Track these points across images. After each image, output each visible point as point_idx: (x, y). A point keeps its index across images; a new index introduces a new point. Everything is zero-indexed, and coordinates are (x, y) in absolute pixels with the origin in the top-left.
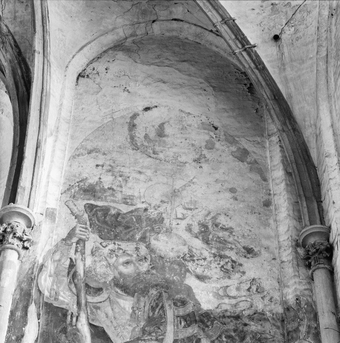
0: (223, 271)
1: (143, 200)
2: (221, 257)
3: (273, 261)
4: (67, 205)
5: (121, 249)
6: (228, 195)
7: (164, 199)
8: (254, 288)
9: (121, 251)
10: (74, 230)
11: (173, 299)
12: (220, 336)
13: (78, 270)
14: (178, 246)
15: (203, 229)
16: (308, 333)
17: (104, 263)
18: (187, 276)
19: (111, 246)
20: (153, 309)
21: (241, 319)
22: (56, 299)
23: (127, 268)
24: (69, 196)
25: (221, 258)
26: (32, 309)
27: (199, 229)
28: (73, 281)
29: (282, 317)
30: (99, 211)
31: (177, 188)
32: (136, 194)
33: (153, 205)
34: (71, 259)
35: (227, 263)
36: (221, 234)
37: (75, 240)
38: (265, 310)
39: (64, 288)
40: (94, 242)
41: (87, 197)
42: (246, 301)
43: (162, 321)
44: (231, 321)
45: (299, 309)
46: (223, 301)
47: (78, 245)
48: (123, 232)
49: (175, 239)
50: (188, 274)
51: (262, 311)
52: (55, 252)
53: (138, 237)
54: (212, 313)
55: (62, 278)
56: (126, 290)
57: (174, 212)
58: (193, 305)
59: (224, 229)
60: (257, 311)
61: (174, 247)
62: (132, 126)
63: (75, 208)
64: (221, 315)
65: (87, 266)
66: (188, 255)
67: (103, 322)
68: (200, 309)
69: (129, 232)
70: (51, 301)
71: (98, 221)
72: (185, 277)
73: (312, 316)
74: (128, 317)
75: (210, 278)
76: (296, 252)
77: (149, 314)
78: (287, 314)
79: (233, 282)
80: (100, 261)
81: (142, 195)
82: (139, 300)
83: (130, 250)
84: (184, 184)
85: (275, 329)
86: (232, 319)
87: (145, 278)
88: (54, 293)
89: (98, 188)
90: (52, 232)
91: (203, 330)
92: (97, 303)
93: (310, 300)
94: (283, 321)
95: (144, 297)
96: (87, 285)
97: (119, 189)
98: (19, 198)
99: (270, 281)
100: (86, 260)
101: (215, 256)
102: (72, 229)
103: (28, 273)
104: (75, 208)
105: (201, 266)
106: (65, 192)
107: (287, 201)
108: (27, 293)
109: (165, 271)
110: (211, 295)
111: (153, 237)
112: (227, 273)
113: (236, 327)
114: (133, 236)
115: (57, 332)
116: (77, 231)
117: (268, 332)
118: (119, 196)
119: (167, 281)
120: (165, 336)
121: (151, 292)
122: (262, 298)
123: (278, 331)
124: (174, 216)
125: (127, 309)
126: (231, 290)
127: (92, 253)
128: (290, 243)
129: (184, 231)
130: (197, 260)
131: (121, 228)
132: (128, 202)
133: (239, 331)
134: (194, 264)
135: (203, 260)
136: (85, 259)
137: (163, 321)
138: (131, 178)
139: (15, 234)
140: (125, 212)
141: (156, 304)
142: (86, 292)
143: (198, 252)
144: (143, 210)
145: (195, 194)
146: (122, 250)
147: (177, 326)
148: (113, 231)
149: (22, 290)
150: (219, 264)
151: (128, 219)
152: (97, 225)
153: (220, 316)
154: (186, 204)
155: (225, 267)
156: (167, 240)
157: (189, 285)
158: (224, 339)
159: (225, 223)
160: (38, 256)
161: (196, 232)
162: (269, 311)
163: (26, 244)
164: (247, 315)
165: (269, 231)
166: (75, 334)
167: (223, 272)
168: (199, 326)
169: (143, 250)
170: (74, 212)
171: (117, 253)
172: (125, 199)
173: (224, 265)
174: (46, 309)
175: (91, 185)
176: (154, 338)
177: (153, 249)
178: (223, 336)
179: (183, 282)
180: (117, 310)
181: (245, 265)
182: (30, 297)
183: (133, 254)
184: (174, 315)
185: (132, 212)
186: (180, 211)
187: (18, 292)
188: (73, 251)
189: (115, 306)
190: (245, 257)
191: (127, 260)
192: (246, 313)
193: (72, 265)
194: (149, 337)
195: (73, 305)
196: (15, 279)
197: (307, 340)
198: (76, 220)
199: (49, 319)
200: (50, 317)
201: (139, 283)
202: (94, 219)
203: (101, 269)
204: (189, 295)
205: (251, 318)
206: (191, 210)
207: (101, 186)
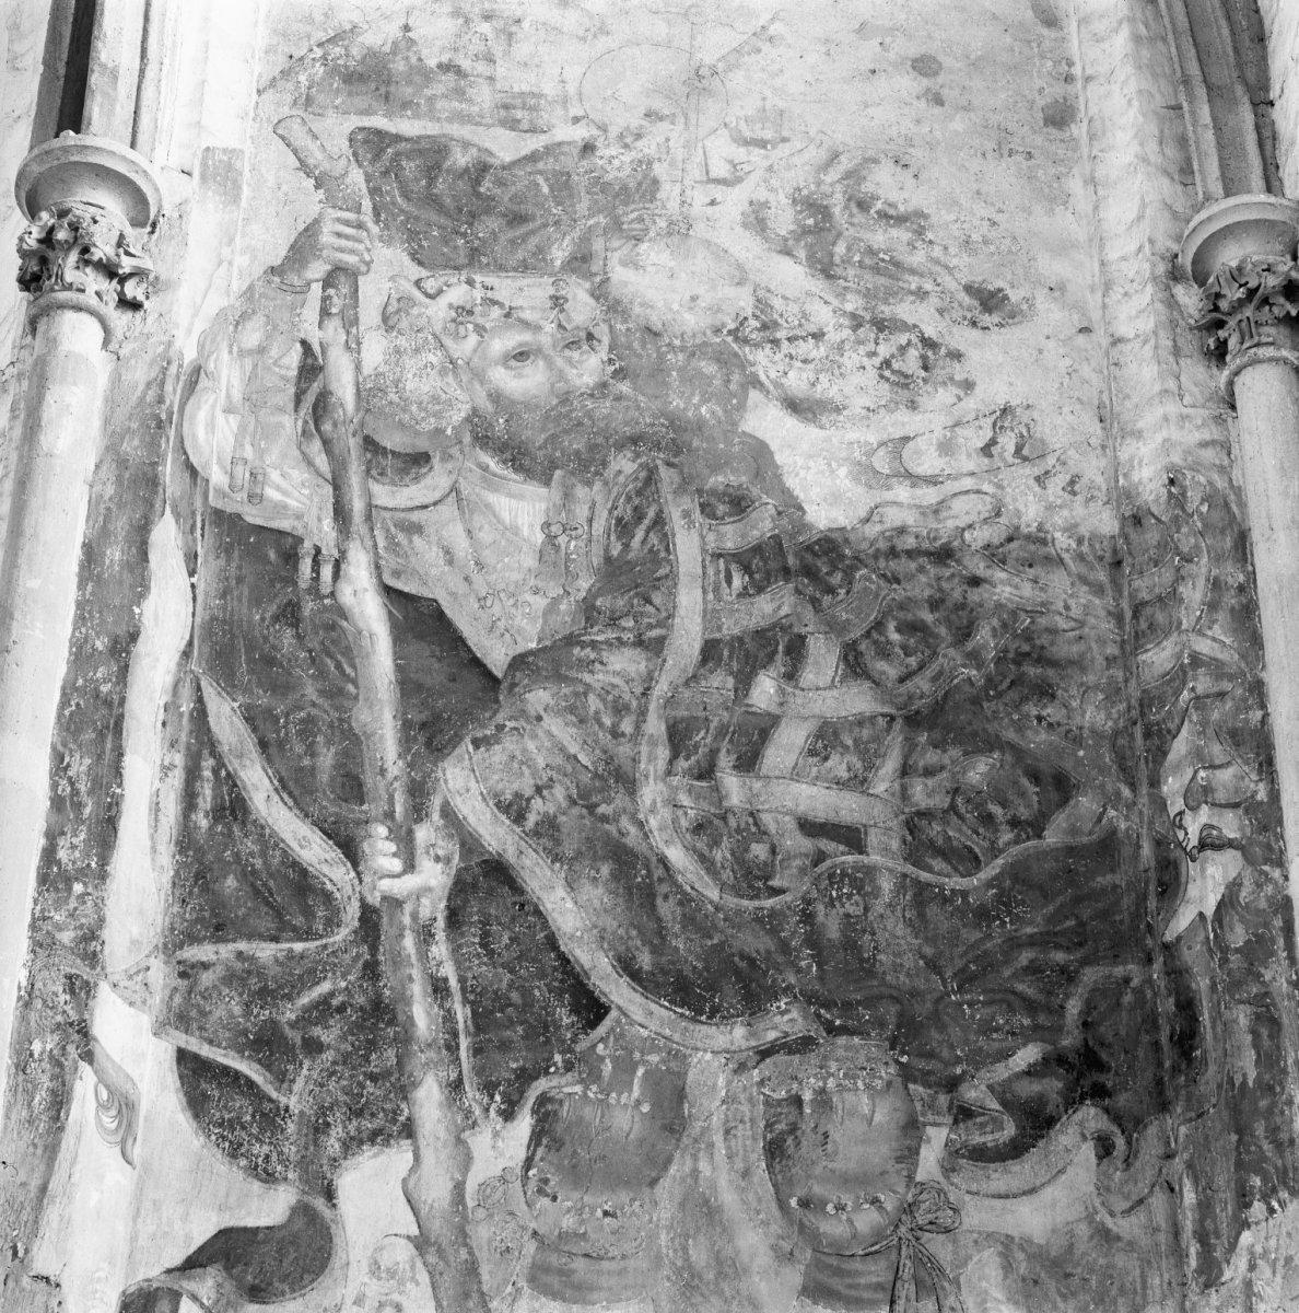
0: (888, 380)
1: (576, 111)
2: (880, 325)
3: (1081, 339)
4: (283, 138)
5: (494, 302)
6: (908, 84)
7: (658, 104)
8: (1008, 442)
9: (496, 312)
10: (311, 231)
11: (700, 492)
12: (879, 626)
13: (333, 387)
14: (714, 288)
15: (811, 222)
16: (1213, 606)
17: (434, 358)
18: (750, 402)
19: (457, 294)
20: (624, 528)
21: (958, 562)
22: (254, 498)
23: (520, 376)
24: (289, 99)
25: (881, 330)
26: (166, 536)
27: (797, 222)
28: (318, 429)
29: (1115, 551)
31: (708, 60)
32: (549, 88)
33: (614, 131)
34: (304, 343)
35: (903, 349)
36: (879, 238)
37: (317, 270)
38: (1048, 526)
39: (284, 456)
40: (392, 279)
41: (361, 102)
42: (978, 492)
43: (658, 574)
44: (921, 569)
45: (1177, 517)
46: (889, 496)
47: (331, 291)
49: (701, 261)
50: (754, 395)
51: (1040, 529)
52: (244, 317)
53: (559, 254)
54: (846, 541)
55: (274, 419)
56: (517, 456)
57: (698, 158)
58: (773, 511)
60: (1017, 528)
61: (701, 291)
63: (313, 146)
64: (882, 545)
65: (367, 369)
66: (754, 323)
67: (434, 580)
68: (802, 526)
69: (525, 238)
70: (237, 504)
71: (406, 196)
72: (742, 407)
73: (1228, 543)
74: (530, 561)
75: (838, 410)
76: (1172, 303)
77: (607, 550)
78: (1133, 536)
80: (417, 351)
81: (571, 89)
82: (567, 495)
83: (533, 308)
84: (735, 45)
85: (1084, 595)
86: (923, 560)
87: (589, 415)
88: (247, 475)
89: (399, 66)
90: (231, 241)
91: (815, 602)
92: (412, 509)
93: (1220, 483)
94: (1118, 564)
95: (589, 484)
96: (370, 444)
97: (481, 67)
98: (95, 109)
99: (1070, 418)
100: (364, 347)
101: (857, 322)
102: (306, 230)
103: (142, 399)
104: (313, 146)
105: (805, 361)
106: (273, 83)
107: (1136, 103)
108: (145, 474)
109: (666, 384)
110: (843, 471)
111: (617, 255)
112: (902, 386)
113: (940, 590)
114: (540, 251)
115: (263, 619)
116: (326, 238)
117: (1060, 606)
118: (483, 97)
119: (675, 422)
120: (670, 628)
121: (614, 467)
122: (1038, 479)
123: (1097, 601)
124: (696, 173)
125: (526, 532)
126: (918, 452)
127: (385, 319)
128: (1147, 266)
129: (739, 230)
130: (789, 339)
131: (493, 223)
132: (519, 121)
133: (949, 604)
134: (778, 356)
135: (811, 341)
136: (359, 344)
137: (661, 572)
138: (526, 24)
139: (85, 250)
140: (508, 159)
141: (636, 509)
142: (368, 471)
143: (794, 308)
144: (575, 152)
145: (778, 82)
146: (501, 305)
147: (716, 590)
148: (464, 235)
149: (122, 463)
150: (873, 354)
151: (519, 186)
152: (402, 211)
153: (878, 550)
155: (896, 365)
156: (673, 264)
157: (759, 435)
158: (895, 637)
159: (894, 196)
160: (180, 334)
161: (783, 233)
162: (1065, 530)
163: (132, 290)
164: (980, 544)
165: (1067, 223)
166: (333, 627)
167: (887, 386)
168: (798, 591)
169: (582, 306)
170: (311, 161)
171: (480, 321)
172: (506, 107)
173: (893, 356)
174: (220, 535)
175: (371, 54)
176: (628, 636)
177: (618, 302)
178: (891, 626)
179: (735, 424)
180: (485, 536)
181: (974, 356)
182: (156, 493)
183: (541, 322)
184: (704, 551)
185: (533, 158)
186: (721, 152)
187: (109, 472)
188: (311, 313)
189: (478, 520)
190: (974, 324)
191: (521, 345)
192: (978, 537)
193: (311, 368)
194: (611, 635)
195: (319, 520)
196: (97, 423)
197: (1210, 633)
198: (321, 194)
199: (233, 571)
200: (234, 565)
201: (566, 432)
202: (390, 187)
203: (420, 381)
204: (758, 475)
205: (993, 553)
206: (765, 147)
207: (414, 60)
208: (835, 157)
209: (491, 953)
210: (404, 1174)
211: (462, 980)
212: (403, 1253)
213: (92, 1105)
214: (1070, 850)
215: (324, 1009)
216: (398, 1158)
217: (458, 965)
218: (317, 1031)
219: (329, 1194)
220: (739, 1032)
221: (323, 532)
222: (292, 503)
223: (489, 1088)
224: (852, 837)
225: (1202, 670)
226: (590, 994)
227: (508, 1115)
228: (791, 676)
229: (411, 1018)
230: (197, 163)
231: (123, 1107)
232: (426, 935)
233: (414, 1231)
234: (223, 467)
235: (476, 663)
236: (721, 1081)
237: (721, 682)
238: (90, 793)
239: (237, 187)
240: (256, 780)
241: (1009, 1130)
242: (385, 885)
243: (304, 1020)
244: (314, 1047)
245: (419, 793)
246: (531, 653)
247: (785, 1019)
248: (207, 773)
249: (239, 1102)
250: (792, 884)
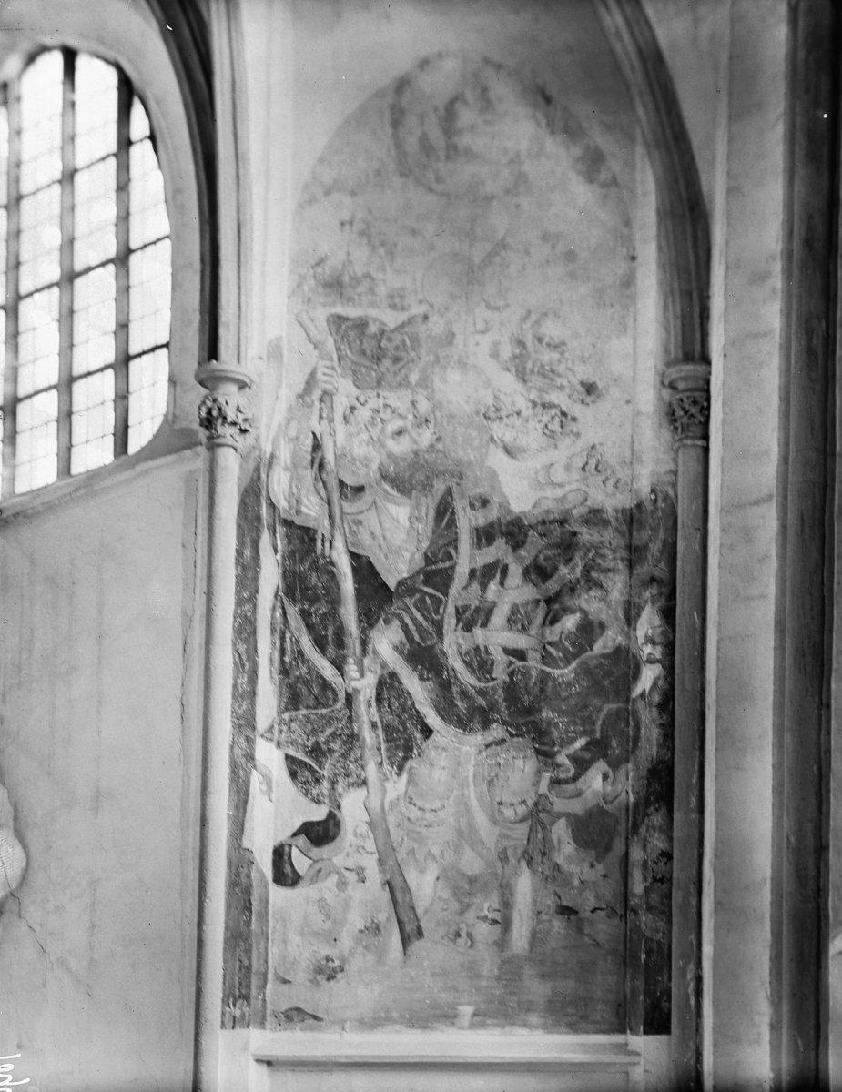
1: (420, 297)
8: (593, 463)
10: (313, 375)
14: (477, 391)
17: (365, 436)
22: (298, 512)
23: (399, 444)
24: (301, 299)
30: (352, 330)
34: (314, 434)
37: (316, 394)
48: (392, 370)
50: (492, 446)
53: (414, 377)
59: (554, 346)
64: (540, 519)
65: (338, 444)
68: (509, 512)
69: (400, 370)
72: (486, 454)
74: (403, 536)
76: (660, 399)
79: (559, 455)
82: (417, 506)
87: (426, 461)
89: (346, 279)
92: (357, 513)
96: (341, 484)
101: (534, 404)
110: (525, 483)
116: (319, 375)
121: (436, 486)
124: (471, 329)
125: (402, 521)
127: (345, 418)
134: (502, 426)
146: (391, 407)
148: (375, 371)
154: (491, 298)
170: (312, 335)
180: (387, 525)
185: (403, 325)
190: (583, 402)
193: (317, 446)
203: (360, 450)
208: (529, 312)
209: (392, 710)
210: (364, 798)
211: (382, 722)
212: (364, 828)
213: (257, 784)
214: (604, 656)
215: (333, 735)
217: (381, 718)
218: (332, 745)
219: (339, 807)
220: (479, 738)
221: (323, 527)
222: (313, 514)
223: (392, 764)
224: (520, 655)
225: (655, 584)
226: (426, 725)
227: (399, 775)
228: (502, 584)
229: (364, 739)
230: (265, 352)
231: (268, 781)
232: (369, 704)
233: (368, 819)
234: (286, 499)
235: (384, 585)
236: (473, 757)
237: (475, 586)
238: (247, 660)
239: (282, 355)
240: (307, 644)
241: (572, 771)
242: (354, 684)
243: (327, 742)
244: (331, 751)
245: (364, 643)
246: (406, 579)
247: (497, 731)
248: (288, 640)
249: (307, 774)
250: (500, 674)
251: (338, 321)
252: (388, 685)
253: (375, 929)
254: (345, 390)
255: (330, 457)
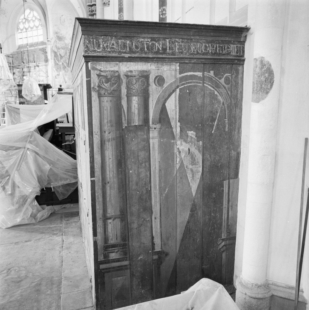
20: (66, 51)
62: (60, 20)
67: (60, 53)
119: (67, 47)
131: (61, 39)
169: (64, 43)
193: (56, 46)
216: (61, 72)
221: (57, 52)
240: (56, 60)
251: (57, 36)
252: (63, 63)
253: (63, 82)
254: (58, 41)
255: (57, 47)
